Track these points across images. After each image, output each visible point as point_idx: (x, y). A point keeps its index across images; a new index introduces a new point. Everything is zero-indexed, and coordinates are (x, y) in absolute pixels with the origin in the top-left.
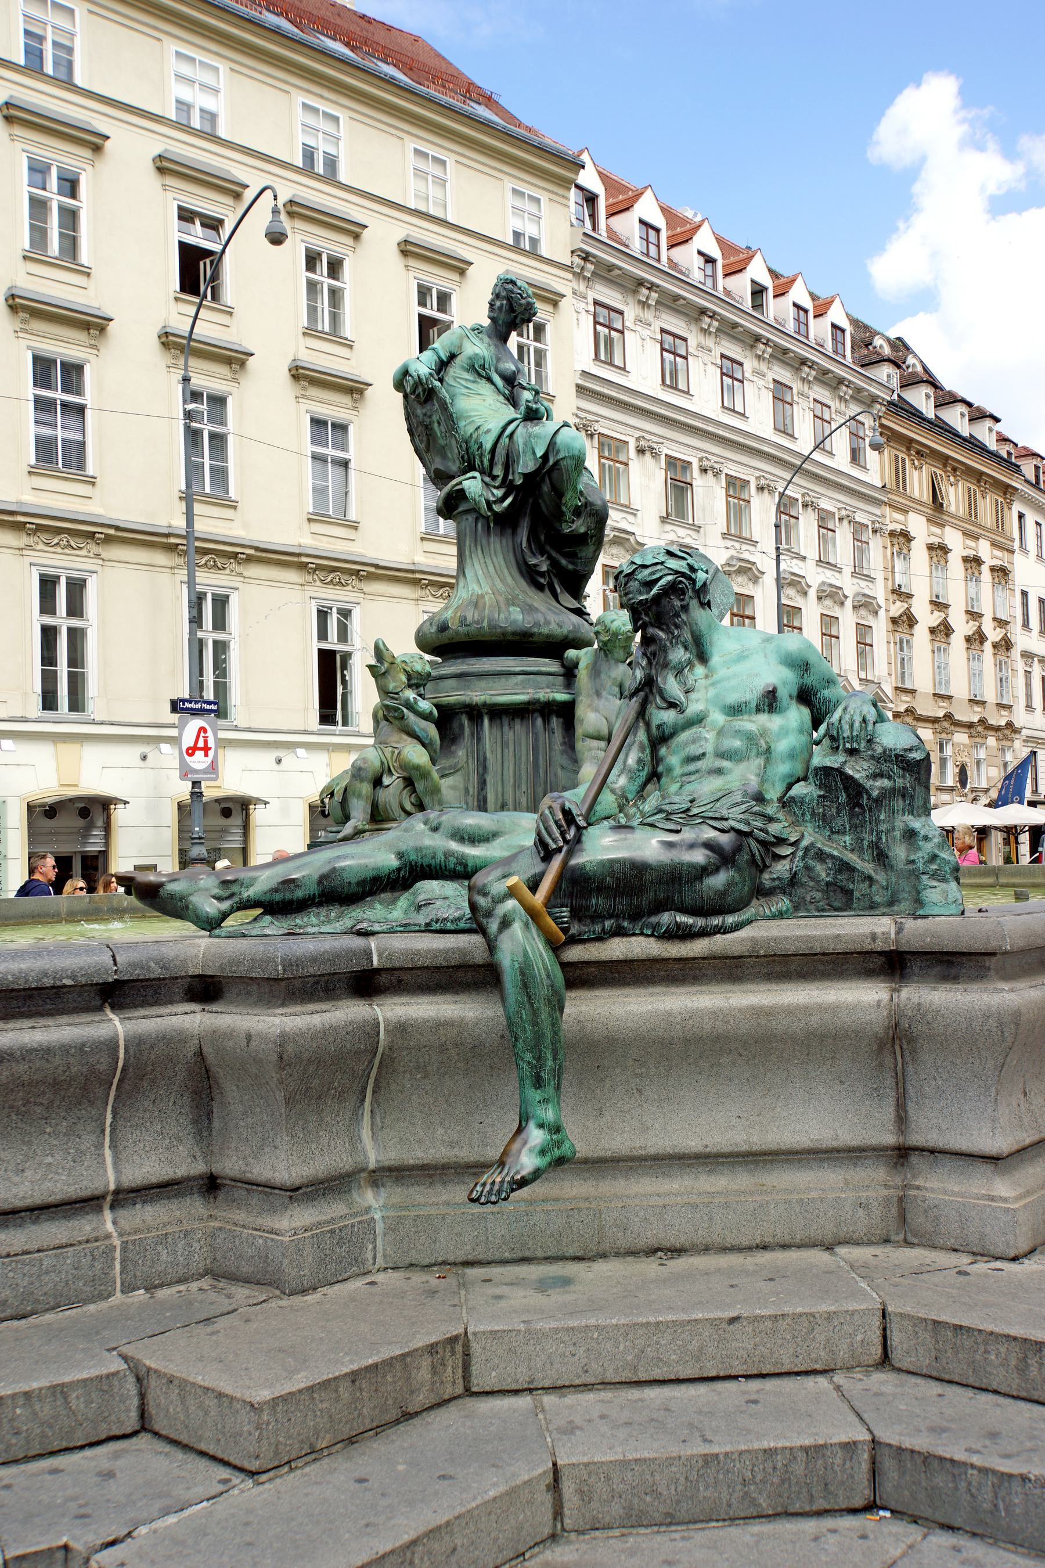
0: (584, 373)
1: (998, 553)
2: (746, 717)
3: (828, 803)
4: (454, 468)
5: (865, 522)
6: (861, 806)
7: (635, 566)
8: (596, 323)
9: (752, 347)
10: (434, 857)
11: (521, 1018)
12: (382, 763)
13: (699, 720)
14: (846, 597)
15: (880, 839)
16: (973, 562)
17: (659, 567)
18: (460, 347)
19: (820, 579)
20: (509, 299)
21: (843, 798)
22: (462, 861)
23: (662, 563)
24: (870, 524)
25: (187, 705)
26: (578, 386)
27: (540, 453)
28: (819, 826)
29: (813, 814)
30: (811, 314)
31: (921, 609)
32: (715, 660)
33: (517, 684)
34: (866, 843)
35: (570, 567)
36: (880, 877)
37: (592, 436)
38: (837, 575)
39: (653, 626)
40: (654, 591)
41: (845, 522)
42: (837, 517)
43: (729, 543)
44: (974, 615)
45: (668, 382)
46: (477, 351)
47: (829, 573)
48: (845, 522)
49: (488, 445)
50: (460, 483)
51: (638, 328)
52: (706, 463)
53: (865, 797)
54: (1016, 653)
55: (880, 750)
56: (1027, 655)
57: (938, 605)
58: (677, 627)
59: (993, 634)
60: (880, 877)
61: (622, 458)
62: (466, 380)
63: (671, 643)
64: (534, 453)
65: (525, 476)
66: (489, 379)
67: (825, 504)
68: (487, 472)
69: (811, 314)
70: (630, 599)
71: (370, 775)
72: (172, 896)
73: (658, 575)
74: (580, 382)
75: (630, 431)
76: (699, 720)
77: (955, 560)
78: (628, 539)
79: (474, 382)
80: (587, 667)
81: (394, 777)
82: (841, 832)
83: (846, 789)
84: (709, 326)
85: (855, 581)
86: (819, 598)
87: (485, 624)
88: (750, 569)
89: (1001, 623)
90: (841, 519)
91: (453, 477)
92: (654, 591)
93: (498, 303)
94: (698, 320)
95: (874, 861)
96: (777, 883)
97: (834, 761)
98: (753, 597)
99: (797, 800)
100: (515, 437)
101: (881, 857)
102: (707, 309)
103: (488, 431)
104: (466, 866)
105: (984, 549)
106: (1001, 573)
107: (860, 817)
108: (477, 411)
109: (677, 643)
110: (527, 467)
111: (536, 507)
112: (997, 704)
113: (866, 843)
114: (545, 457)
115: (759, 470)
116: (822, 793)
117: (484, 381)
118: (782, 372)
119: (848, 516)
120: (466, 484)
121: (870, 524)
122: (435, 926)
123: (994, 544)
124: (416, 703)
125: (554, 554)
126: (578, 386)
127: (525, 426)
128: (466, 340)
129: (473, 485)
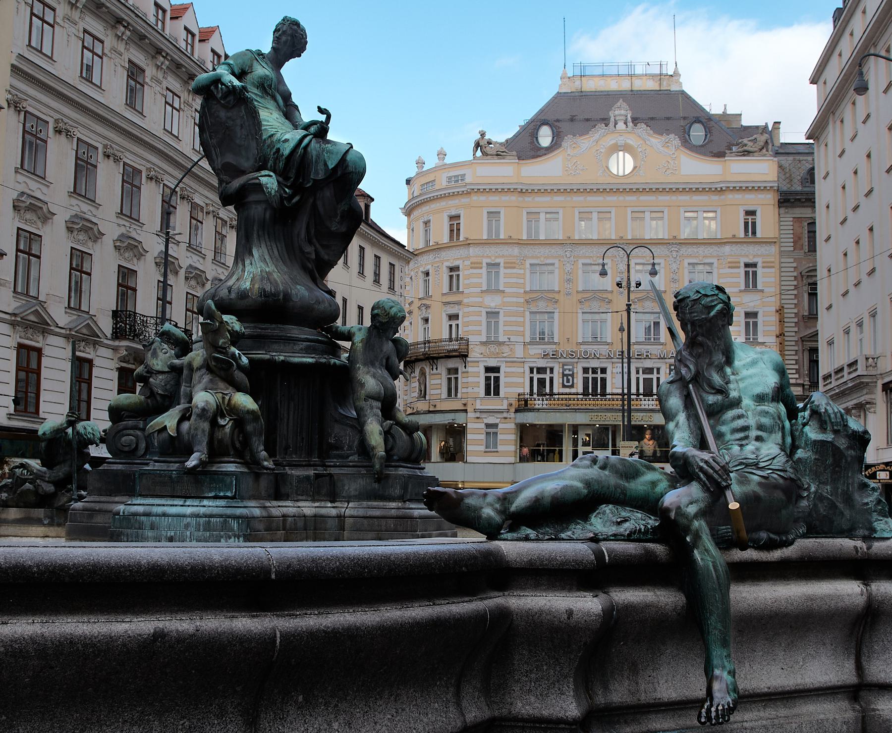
0: (20, 56)
2: (766, 404)
3: (819, 464)
4: (246, 164)
5: (226, 218)
6: (840, 467)
7: (700, 295)
8: (32, 14)
9: (153, 57)
10: (608, 488)
11: (716, 599)
12: (217, 405)
13: (737, 403)
14: (208, 280)
15: (848, 488)
17: (715, 298)
18: (251, 66)
19: (189, 262)
20: (293, 36)
21: (830, 461)
22: (624, 491)
23: (717, 295)
24: (228, 220)
26: (13, 66)
27: (331, 166)
28: (813, 479)
29: (810, 471)
30: (197, 38)
32: (737, 363)
33: (301, 349)
34: (840, 490)
35: (326, 257)
36: (847, 513)
37: (19, 111)
38: (201, 260)
39: (703, 335)
40: (712, 314)
41: (211, 216)
42: (205, 211)
43: (122, 222)
45: (84, 75)
46: (267, 73)
47: (195, 258)
48: (211, 216)
49: (286, 152)
50: (257, 178)
51: (66, 25)
52: (110, 151)
53: (844, 461)
55: (850, 432)
58: (719, 339)
60: (847, 513)
61: (42, 136)
62: (256, 94)
63: (715, 348)
64: (326, 164)
65: (314, 180)
66: (274, 98)
67: (198, 200)
68: (283, 175)
69: (197, 38)
70: (694, 316)
71: (210, 414)
72: (469, 507)
73: (715, 303)
74: (15, 63)
75: (52, 113)
76: (737, 403)
78: (41, 208)
79: (262, 97)
80: (362, 341)
81: (228, 419)
82: (825, 483)
83: (834, 455)
84: (123, 34)
85: (214, 267)
86: (187, 278)
87: (281, 297)
88: (136, 246)
90: (208, 213)
91: (243, 172)
92: (712, 314)
93: (284, 38)
94: (114, 27)
95: (843, 503)
96: (800, 515)
97: (829, 437)
98: (136, 271)
99: (803, 460)
100: (309, 149)
101: (848, 500)
102: (123, 19)
103: (286, 141)
104: (625, 495)
107: (838, 474)
108: (268, 121)
109: (718, 350)
110: (318, 174)
111: (314, 206)
113: (840, 490)
114: (335, 169)
115: (148, 161)
116: (817, 457)
117: (269, 98)
118: (174, 83)
119: (213, 212)
120: (264, 180)
121: (228, 220)
122: (635, 536)
124: (240, 358)
125: (318, 245)
126: (13, 66)
127: (317, 142)
128: (255, 63)
129: (269, 181)
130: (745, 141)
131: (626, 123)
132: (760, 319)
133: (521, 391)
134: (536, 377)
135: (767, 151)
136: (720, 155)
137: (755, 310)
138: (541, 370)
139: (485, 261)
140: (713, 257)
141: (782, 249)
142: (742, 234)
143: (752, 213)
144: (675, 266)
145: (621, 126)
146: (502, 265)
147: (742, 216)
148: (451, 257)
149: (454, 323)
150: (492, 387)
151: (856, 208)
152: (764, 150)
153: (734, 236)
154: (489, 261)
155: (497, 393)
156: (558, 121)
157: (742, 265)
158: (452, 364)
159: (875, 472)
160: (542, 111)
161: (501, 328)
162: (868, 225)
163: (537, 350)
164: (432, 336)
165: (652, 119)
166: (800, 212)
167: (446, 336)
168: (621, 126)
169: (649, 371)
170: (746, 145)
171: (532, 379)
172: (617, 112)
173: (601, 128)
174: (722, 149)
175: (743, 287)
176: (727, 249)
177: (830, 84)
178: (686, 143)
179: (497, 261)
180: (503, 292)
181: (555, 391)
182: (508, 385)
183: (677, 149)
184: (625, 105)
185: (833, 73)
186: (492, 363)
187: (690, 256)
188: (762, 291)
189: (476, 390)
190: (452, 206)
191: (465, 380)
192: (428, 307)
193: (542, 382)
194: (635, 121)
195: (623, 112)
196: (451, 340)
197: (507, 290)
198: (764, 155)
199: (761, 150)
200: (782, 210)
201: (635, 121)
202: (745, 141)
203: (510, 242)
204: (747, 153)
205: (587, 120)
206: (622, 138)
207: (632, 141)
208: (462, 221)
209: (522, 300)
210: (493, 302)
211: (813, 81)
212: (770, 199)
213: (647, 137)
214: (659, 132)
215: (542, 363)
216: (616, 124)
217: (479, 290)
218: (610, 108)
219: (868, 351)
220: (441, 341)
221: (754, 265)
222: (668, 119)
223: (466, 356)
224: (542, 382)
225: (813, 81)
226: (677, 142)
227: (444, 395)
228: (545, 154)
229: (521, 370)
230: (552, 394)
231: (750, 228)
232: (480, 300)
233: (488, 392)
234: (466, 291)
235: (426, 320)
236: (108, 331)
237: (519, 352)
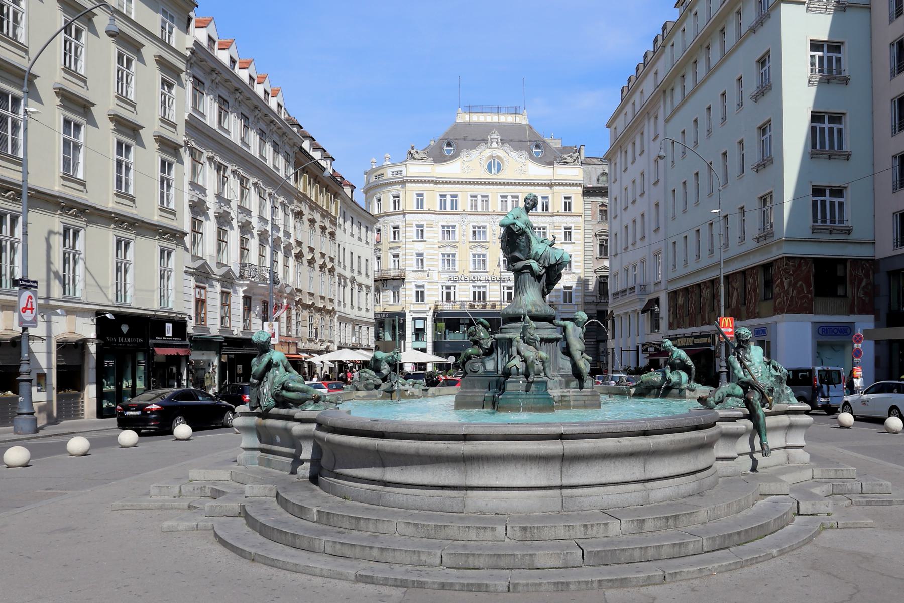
1: (332, 226)
14: (282, 242)
16: (323, 228)
25: (24, 283)
31: (305, 251)
44: (323, 255)
54: (336, 273)
56: (340, 276)
57: (312, 250)
59: (330, 266)
77: (317, 225)
89: (332, 260)
105: (327, 224)
106: (332, 234)
112: (329, 299)
123: (331, 222)
130: (565, 156)
131: (497, 143)
133: (436, 299)
134: (445, 291)
135: (578, 162)
136: (551, 164)
138: (448, 288)
139: (415, 223)
141: (586, 219)
142: (563, 211)
143: (569, 198)
145: (494, 144)
146: (425, 225)
148: (396, 220)
149: (396, 259)
150: (420, 296)
151: (634, 202)
152: (576, 161)
154: (417, 223)
155: (422, 300)
156: (456, 139)
157: (563, 228)
158: (395, 283)
159: (647, 348)
160: (447, 133)
161: (425, 262)
162: (641, 212)
163: (445, 276)
164: (383, 267)
165: (511, 141)
166: (599, 199)
167: (392, 266)
168: (494, 144)
170: (565, 159)
171: (443, 292)
172: (492, 137)
173: (483, 146)
174: (552, 160)
177: (619, 131)
178: (531, 157)
179: (422, 223)
180: (425, 241)
181: (457, 299)
182: (429, 296)
185: (621, 124)
186: (420, 283)
188: (574, 243)
189: (410, 299)
190: (396, 190)
191: (404, 293)
192: (380, 250)
193: (448, 294)
195: (495, 136)
196: (395, 269)
197: (428, 240)
198: (576, 165)
199: (574, 162)
202: (565, 156)
203: (430, 212)
205: (474, 140)
206: (494, 152)
207: (501, 153)
208: (401, 199)
209: (437, 246)
210: (420, 247)
211: (608, 126)
212: (580, 190)
213: (509, 152)
214: (517, 149)
215: (450, 284)
216: (492, 143)
217: (411, 240)
219: (639, 281)
220: (390, 270)
221: (570, 228)
222: (521, 141)
223: (404, 279)
224: (448, 294)
225: (608, 126)
226: (527, 155)
227: (392, 302)
228: (450, 160)
229: (437, 287)
230: (454, 301)
231: (568, 206)
232: (412, 246)
233: (417, 300)
234: (404, 240)
235: (379, 258)
236: (238, 275)
237: (435, 276)
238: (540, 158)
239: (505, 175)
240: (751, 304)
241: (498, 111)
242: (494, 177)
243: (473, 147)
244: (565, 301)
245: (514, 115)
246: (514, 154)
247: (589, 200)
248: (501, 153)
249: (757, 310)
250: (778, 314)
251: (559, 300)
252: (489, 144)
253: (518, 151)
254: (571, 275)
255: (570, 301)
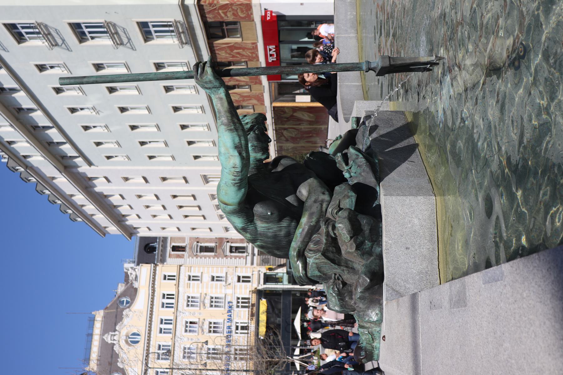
131: (115, 335)
132: (215, 275)
137: (210, 276)
140: (184, 296)
142: (174, 282)
143: (165, 276)
144: (187, 314)
147: (167, 281)
153: (175, 285)
157: (189, 282)
168: (115, 338)
169: (237, 328)
173: (116, 348)
174: (133, 290)
175: (199, 282)
176: (180, 289)
183: (130, 310)
184: (106, 335)
187: (183, 306)
194: (115, 330)
200: (165, 263)
201: (115, 330)
204: (136, 277)
205: (112, 357)
206: (122, 338)
214: (121, 319)
216: (114, 340)
218: (107, 343)
221: (190, 277)
231: (171, 278)
238: (131, 300)
239: (143, 330)
240: (244, 53)
241: (90, 335)
242: (142, 339)
243: (117, 356)
244: (249, 281)
245: (96, 322)
246: (126, 321)
247: (168, 259)
248: (124, 332)
249: (250, 46)
250: (252, 14)
251: (248, 286)
252: (115, 342)
253: (123, 318)
254: (228, 276)
255: (249, 277)
